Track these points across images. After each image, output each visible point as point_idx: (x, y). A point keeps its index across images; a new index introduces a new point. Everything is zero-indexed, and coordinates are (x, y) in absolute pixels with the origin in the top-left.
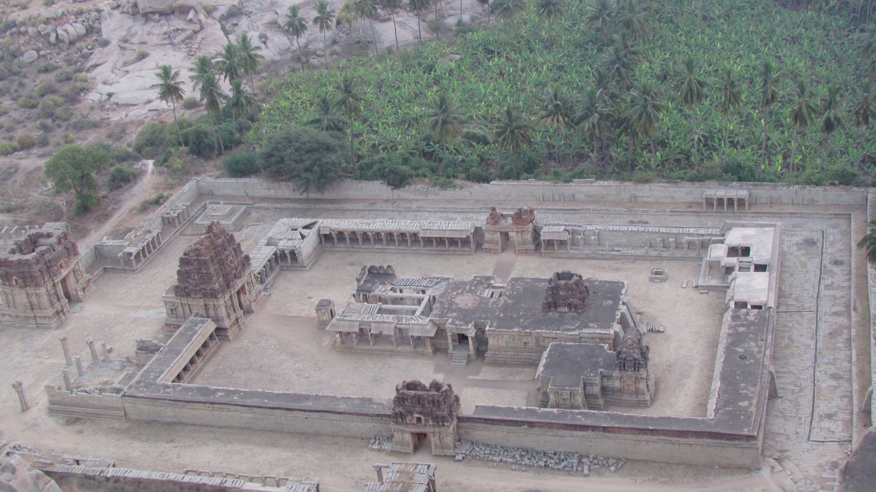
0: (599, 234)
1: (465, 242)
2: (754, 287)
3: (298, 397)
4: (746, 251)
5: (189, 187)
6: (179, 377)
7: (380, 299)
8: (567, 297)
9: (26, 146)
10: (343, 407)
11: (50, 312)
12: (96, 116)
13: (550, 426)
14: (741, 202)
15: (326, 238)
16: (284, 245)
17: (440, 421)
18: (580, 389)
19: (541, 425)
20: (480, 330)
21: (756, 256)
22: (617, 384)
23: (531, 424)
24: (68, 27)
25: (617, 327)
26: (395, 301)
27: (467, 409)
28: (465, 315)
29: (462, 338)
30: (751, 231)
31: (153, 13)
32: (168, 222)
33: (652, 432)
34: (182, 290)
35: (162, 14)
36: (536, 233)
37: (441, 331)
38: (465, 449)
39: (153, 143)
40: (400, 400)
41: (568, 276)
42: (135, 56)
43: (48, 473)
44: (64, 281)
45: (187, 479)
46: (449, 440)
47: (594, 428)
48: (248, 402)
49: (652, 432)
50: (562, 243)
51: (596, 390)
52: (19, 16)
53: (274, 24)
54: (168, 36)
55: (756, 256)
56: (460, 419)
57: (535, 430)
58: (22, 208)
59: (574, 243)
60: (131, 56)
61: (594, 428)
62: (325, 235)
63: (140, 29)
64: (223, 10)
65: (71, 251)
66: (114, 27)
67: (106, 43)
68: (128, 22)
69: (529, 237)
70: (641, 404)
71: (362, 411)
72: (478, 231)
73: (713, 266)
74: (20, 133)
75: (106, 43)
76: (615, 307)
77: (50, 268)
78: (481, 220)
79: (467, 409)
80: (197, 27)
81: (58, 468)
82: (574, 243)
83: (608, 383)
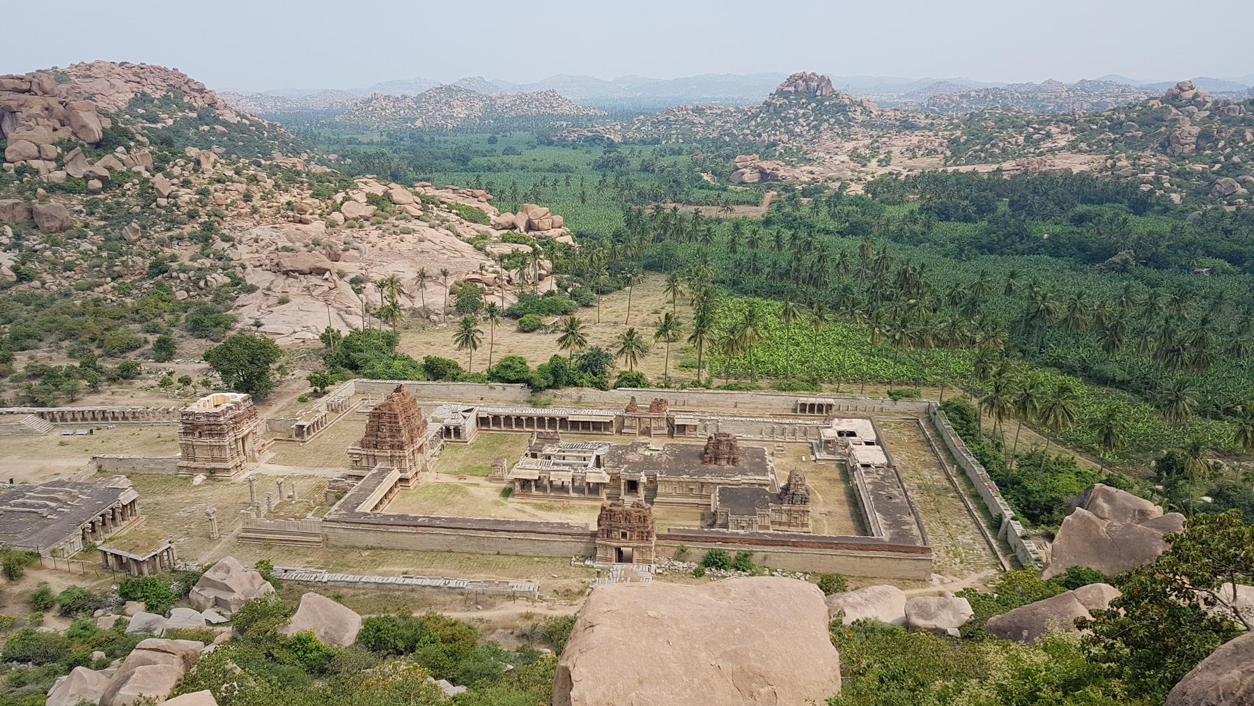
16: (451, 423)
24: (214, 275)
28: (635, 466)
31: (294, 271)
35: (302, 273)
37: (615, 479)
42: (276, 300)
44: (243, 439)
48: (452, 525)
60: (273, 300)
62: (482, 418)
63: (281, 281)
67: (251, 289)
75: (251, 289)
80: (332, 285)
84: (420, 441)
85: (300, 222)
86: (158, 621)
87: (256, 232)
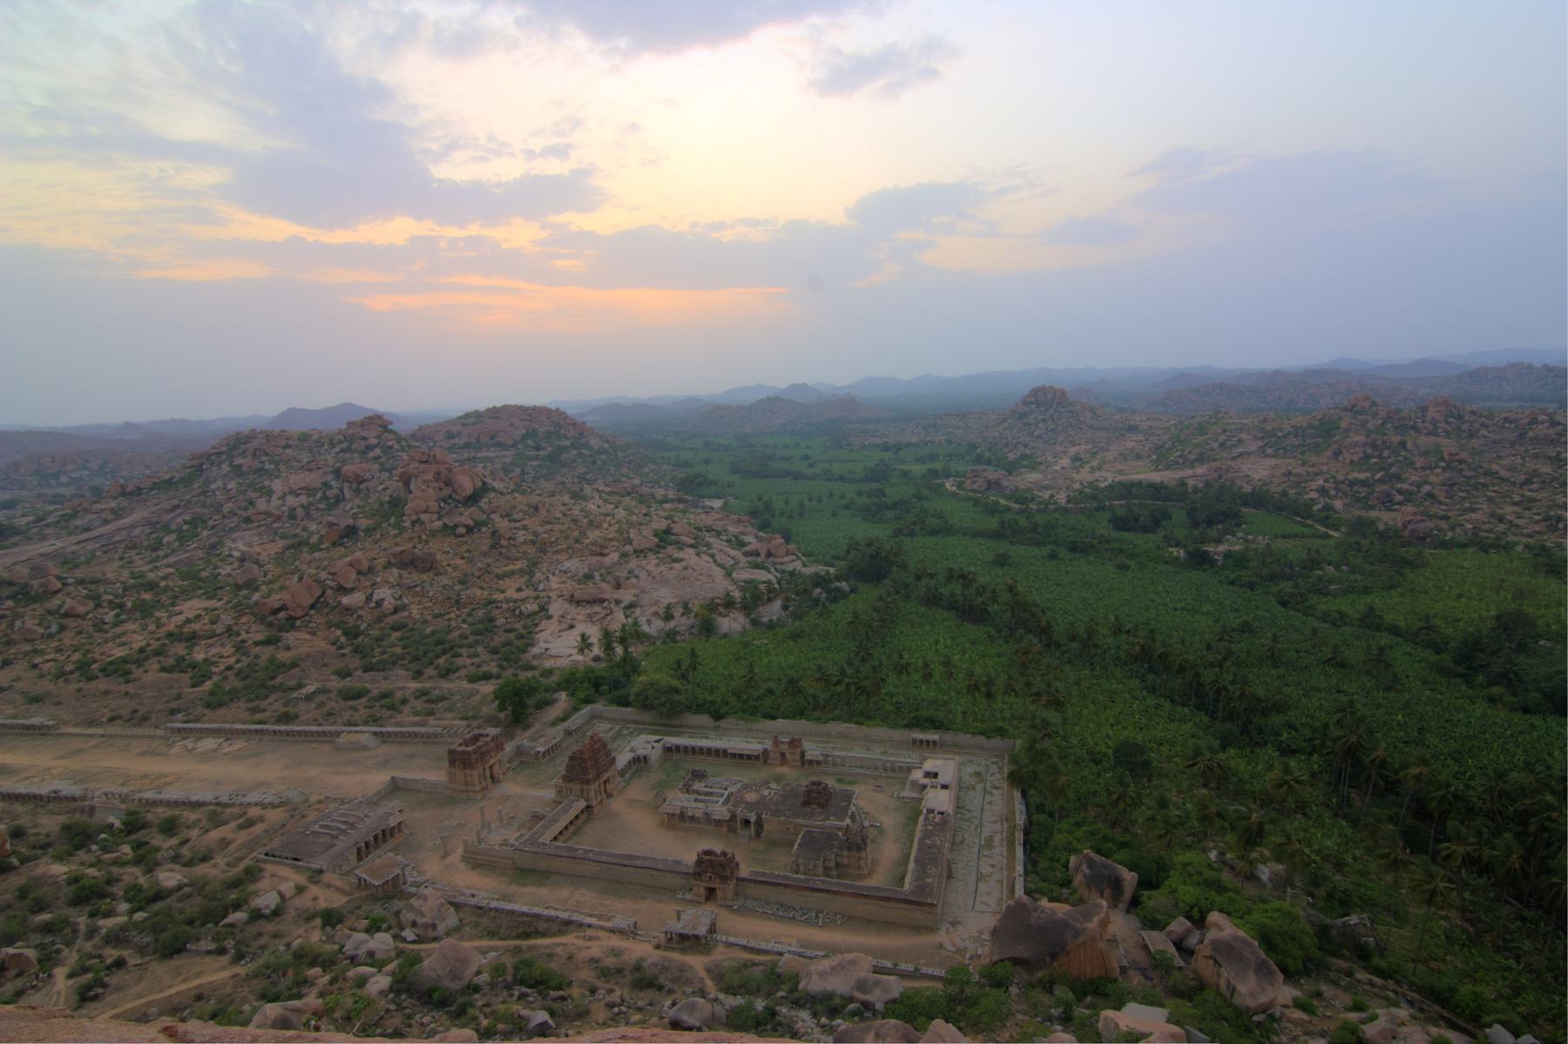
0: (843, 758)
1: (757, 758)
2: (940, 800)
3: (632, 857)
4: (936, 775)
5: (586, 710)
6: (555, 839)
7: (697, 792)
8: (817, 798)
9: (487, 677)
10: (660, 866)
11: (478, 788)
12: (534, 663)
13: (798, 888)
14: (935, 743)
15: (668, 750)
16: (641, 752)
17: (725, 879)
18: (820, 863)
19: (792, 887)
20: (759, 817)
21: (941, 780)
22: (846, 861)
23: (786, 886)
25: (848, 821)
26: (707, 794)
27: (744, 871)
28: (750, 806)
29: (747, 823)
30: (939, 762)
32: (569, 733)
33: (866, 896)
34: (567, 779)
36: (803, 754)
37: (733, 817)
38: (740, 902)
39: (570, 681)
40: (699, 862)
41: (819, 783)
43: (451, 903)
45: (546, 912)
46: (730, 894)
47: (827, 891)
49: (866, 896)
50: (819, 763)
51: (832, 864)
52: (500, 597)
53: (656, 614)
54: (590, 616)
55: (941, 780)
56: (739, 879)
57: (789, 891)
58: (475, 717)
59: (826, 763)
61: (827, 891)
63: (573, 610)
64: (626, 603)
65: (500, 747)
66: (556, 608)
68: (566, 605)
69: (798, 757)
70: (861, 877)
71: (673, 869)
72: (765, 751)
73: (914, 783)
74: (485, 668)
75: (550, 618)
76: (847, 807)
77: (483, 757)
78: (768, 744)
79: (744, 871)
81: (460, 899)
82: (826, 763)
83: (840, 860)
84: (606, 776)
85: (601, 554)
86: (365, 942)
87: (567, 564)
